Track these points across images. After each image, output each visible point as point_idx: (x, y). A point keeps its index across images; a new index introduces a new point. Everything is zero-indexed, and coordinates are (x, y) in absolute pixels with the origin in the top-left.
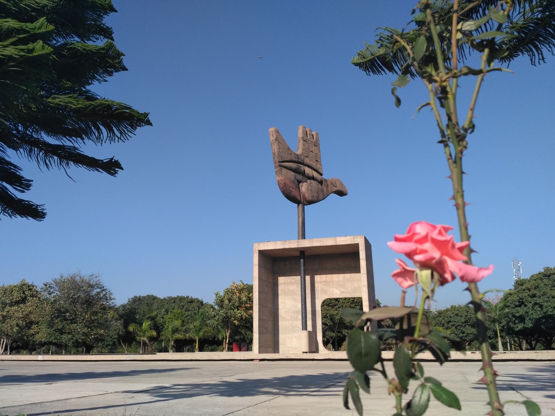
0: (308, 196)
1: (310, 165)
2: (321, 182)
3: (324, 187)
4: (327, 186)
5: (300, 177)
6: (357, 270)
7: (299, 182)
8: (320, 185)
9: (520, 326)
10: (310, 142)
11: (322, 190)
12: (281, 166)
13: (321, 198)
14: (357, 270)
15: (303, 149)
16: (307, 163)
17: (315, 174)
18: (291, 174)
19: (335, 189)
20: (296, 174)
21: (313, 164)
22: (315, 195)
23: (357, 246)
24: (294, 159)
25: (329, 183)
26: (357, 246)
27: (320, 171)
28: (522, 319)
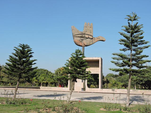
5: (82, 39)
6: (98, 66)
9: (141, 83)
11: (92, 41)
13: (91, 44)
14: (98, 66)
17: (90, 37)
18: (79, 38)
19: (99, 40)
21: (89, 34)
22: (88, 43)
23: (99, 60)
24: (80, 34)
26: (99, 60)
28: (142, 81)
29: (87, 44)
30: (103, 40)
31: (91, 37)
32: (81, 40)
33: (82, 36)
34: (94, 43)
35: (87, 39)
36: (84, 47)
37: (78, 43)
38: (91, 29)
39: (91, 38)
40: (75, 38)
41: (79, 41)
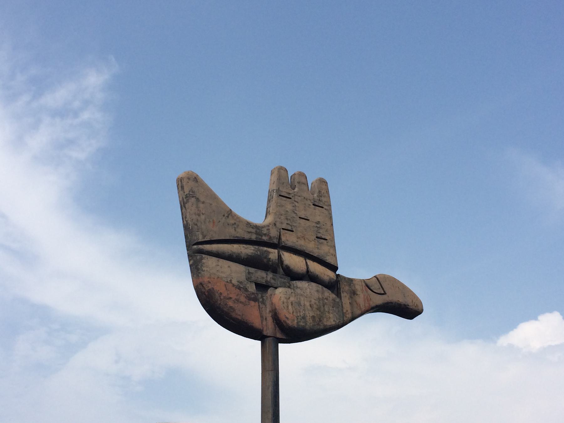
0: (290, 316)
1: (299, 248)
4: (354, 293)
5: (261, 275)
7: (263, 287)
8: (328, 293)
10: (297, 198)
11: (338, 305)
13: (331, 322)
17: (316, 268)
18: (237, 272)
19: (379, 300)
20: (252, 270)
21: (311, 247)
22: (310, 314)
24: (247, 237)
25: (358, 287)
27: (329, 259)
29: (304, 318)
30: (411, 305)
32: (252, 288)
34: (349, 316)
35: (299, 284)
37: (230, 303)
38: (317, 215)
39: (326, 278)
40: (210, 263)
41: (240, 287)
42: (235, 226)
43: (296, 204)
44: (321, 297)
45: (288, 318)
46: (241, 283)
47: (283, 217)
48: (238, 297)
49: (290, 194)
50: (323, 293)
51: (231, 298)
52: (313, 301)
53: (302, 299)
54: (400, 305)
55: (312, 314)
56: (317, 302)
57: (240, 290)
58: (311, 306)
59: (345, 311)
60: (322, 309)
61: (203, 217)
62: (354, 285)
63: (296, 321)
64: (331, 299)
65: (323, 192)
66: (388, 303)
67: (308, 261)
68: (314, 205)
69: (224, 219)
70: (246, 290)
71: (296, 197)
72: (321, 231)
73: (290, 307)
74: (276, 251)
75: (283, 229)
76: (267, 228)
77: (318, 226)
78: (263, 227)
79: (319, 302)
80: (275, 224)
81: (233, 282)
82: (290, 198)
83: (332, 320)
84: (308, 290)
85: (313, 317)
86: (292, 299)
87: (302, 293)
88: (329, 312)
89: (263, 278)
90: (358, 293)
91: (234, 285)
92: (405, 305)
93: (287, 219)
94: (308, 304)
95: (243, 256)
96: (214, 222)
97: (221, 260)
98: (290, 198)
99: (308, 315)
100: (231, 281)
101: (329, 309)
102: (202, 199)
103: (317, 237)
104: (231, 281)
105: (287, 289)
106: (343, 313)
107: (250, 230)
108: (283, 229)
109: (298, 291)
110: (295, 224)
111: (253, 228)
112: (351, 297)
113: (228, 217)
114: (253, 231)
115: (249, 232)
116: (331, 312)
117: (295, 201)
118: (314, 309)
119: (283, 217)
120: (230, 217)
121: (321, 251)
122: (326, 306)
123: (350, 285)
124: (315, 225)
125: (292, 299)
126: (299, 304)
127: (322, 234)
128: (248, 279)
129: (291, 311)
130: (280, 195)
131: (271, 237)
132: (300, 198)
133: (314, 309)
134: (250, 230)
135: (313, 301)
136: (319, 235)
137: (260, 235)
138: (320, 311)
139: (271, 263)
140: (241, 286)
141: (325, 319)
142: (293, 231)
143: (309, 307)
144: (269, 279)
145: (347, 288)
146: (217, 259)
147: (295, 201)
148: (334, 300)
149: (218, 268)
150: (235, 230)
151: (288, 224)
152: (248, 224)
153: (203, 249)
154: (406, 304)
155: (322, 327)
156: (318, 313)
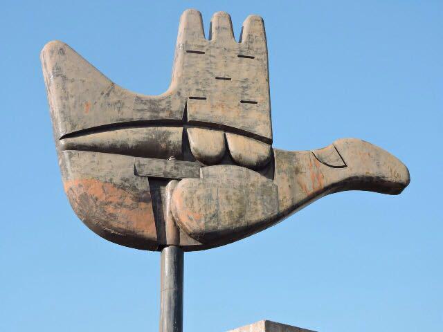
1: (214, 121)
2: (265, 167)
3: (281, 180)
5: (155, 166)
8: (257, 178)
12: (70, 147)
15: (184, 79)
16: (199, 118)
18: (123, 165)
20: (143, 160)
21: (231, 117)
22: (225, 209)
24: (137, 117)
25: (304, 163)
30: (390, 177)
31: (257, 151)
33: (157, 144)
35: (212, 169)
36: (179, 251)
37: (110, 209)
38: (244, 70)
42: (119, 105)
43: (212, 59)
44: (243, 183)
45: (191, 220)
46: (127, 180)
47: (191, 82)
48: (120, 201)
49: (203, 46)
50: (248, 177)
51: (111, 202)
52: (231, 191)
53: (215, 190)
54: (371, 178)
55: (228, 209)
56: (237, 192)
57: (125, 190)
58: (227, 198)
59: (281, 198)
60: (246, 199)
61: (72, 100)
62: (298, 160)
63: (203, 222)
64: (259, 185)
65: (254, 35)
66: (350, 179)
67: (228, 135)
68: (239, 56)
69: (102, 99)
70: (135, 188)
71: (212, 49)
72: (248, 92)
73: (196, 204)
74: (181, 129)
75: (191, 98)
76: (167, 100)
77: (245, 85)
78: (160, 100)
79: (240, 191)
80: (179, 94)
81: (114, 181)
82: (203, 53)
83: (260, 213)
84: (225, 177)
85: (231, 213)
86: (200, 192)
87: (215, 182)
88: (255, 203)
89: (160, 169)
90: (303, 170)
91: (115, 185)
92: (378, 178)
93: (197, 83)
94: (222, 197)
95: (131, 144)
96: (87, 105)
97: (98, 154)
98: (203, 53)
99: (223, 212)
100: (111, 179)
101: (256, 200)
102: (70, 77)
103: (242, 102)
104: (111, 179)
105: (191, 179)
106: (278, 201)
107: (141, 107)
108: (191, 98)
109: (210, 180)
110: (208, 89)
111: (145, 104)
112: (292, 178)
113: (108, 94)
114: (146, 107)
115: (139, 110)
116: (259, 202)
117: (210, 56)
118: (233, 202)
119: (191, 82)
120: (112, 94)
121: (254, 120)
122: (250, 196)
123: (290, 162)
124: (238, 84)
125: (198, 193)
126: (209, 197)
127: (251, 94)
128: (136, 173)
129: (197, 209)
130: (188, 52)
131: (171, 112)
132: (218, 51)
133: (233, 202)
134: (141, 107)
135: (231, 191)
136: (246, 98)
137: (156, 112)
138: (241, 203)
139: (171, 147)
140: (127, 184)
141: (248, 214)
142: (205, 99)
143: (225, 201)
144: (168, 169)
145: (285, 166)
146: (93, 153)
147: (210, 56)
148: (264, 185)
149: (94, 165)
150: (119, 111)
151: (198, 90)
152: (139, 100)
153: (73, 144)
154: (379, 175)
155: (243, 223)
156: (238, 206)
